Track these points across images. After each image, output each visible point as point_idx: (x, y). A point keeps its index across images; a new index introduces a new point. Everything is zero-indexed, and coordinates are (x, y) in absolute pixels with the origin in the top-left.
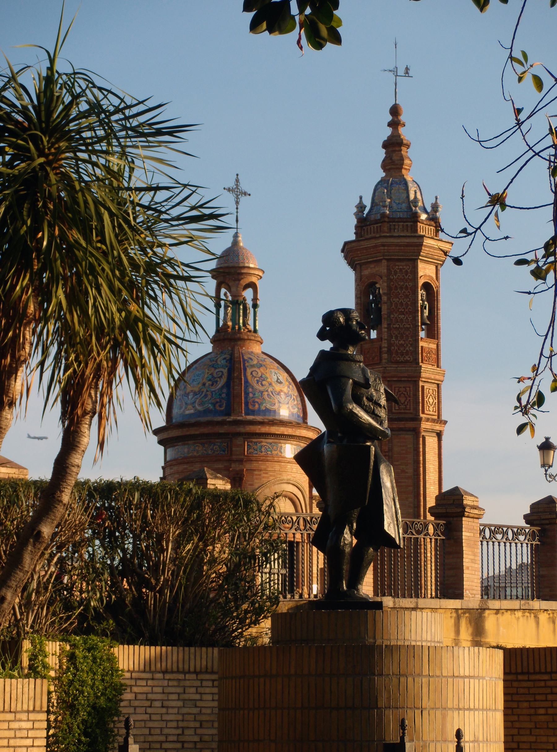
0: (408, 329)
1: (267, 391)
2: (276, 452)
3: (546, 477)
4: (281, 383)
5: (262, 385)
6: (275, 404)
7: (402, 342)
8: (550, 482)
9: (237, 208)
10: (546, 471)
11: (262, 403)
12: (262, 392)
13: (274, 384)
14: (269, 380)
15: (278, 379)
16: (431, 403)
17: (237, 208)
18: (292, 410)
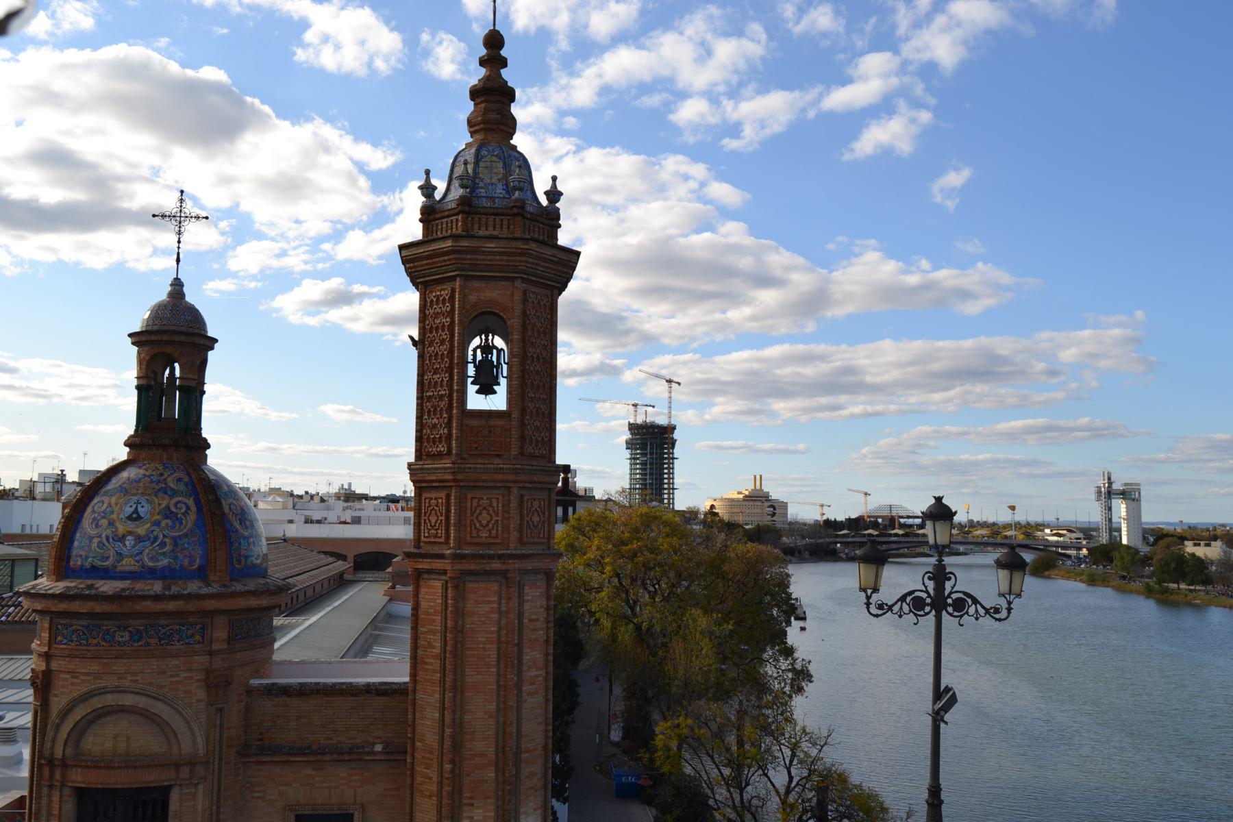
0: (441, 397)
1: (100, 536)
2: (96, 641)
3: (868, 608)
4: (139, 518)
5: (97, 526)
6: (107, 558)
7: (435, 421)
8: (877, 616)
9: (179, 242)
10: (868, 598)
11: (87, 557)
12: (91, 538)
13: (118, 524)
14: (114, 516)
15: (136, 511)
16: (484, 522)
17: (179, 242)
18: (150, 564)
